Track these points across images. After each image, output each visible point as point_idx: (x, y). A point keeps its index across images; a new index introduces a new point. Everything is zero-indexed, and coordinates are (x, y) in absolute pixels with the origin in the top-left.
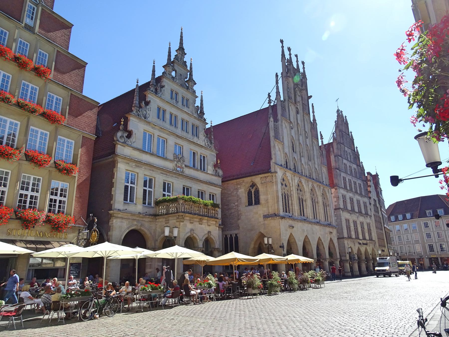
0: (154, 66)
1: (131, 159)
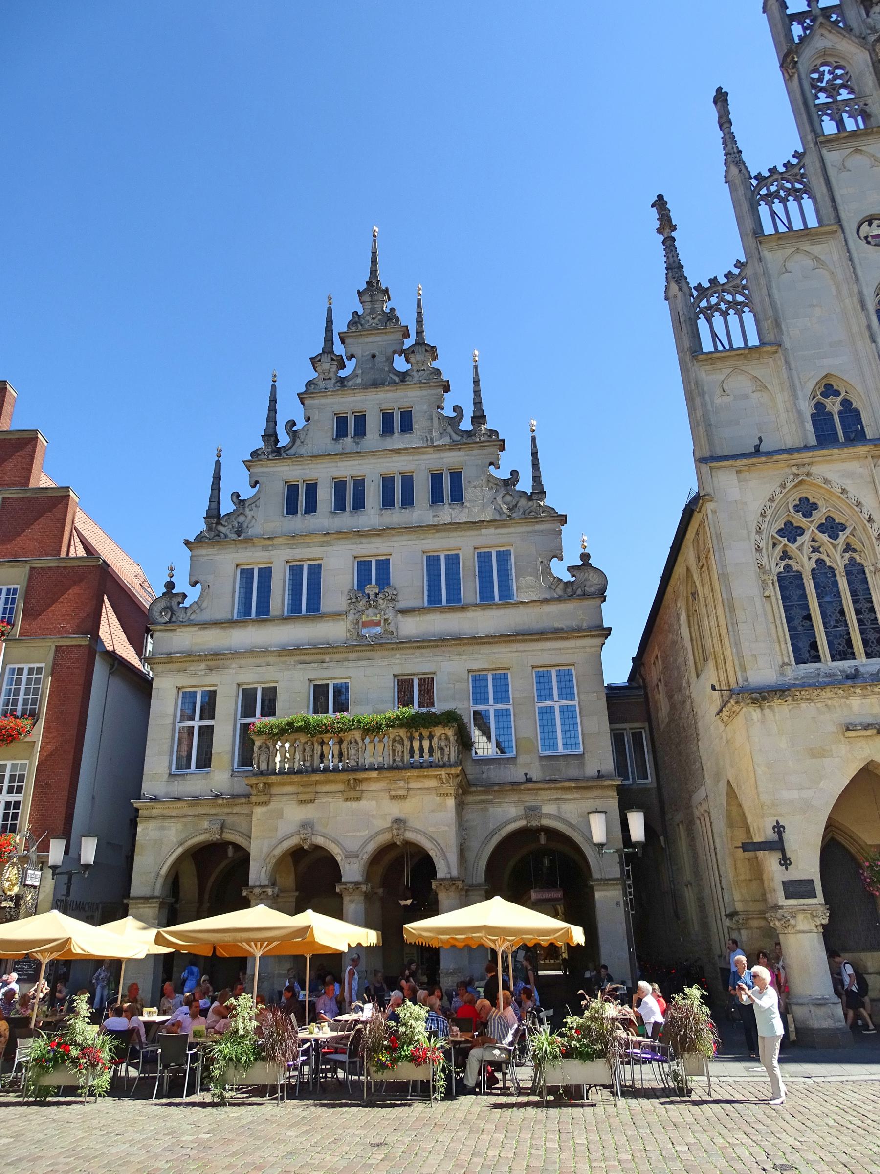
1: (189, 656)
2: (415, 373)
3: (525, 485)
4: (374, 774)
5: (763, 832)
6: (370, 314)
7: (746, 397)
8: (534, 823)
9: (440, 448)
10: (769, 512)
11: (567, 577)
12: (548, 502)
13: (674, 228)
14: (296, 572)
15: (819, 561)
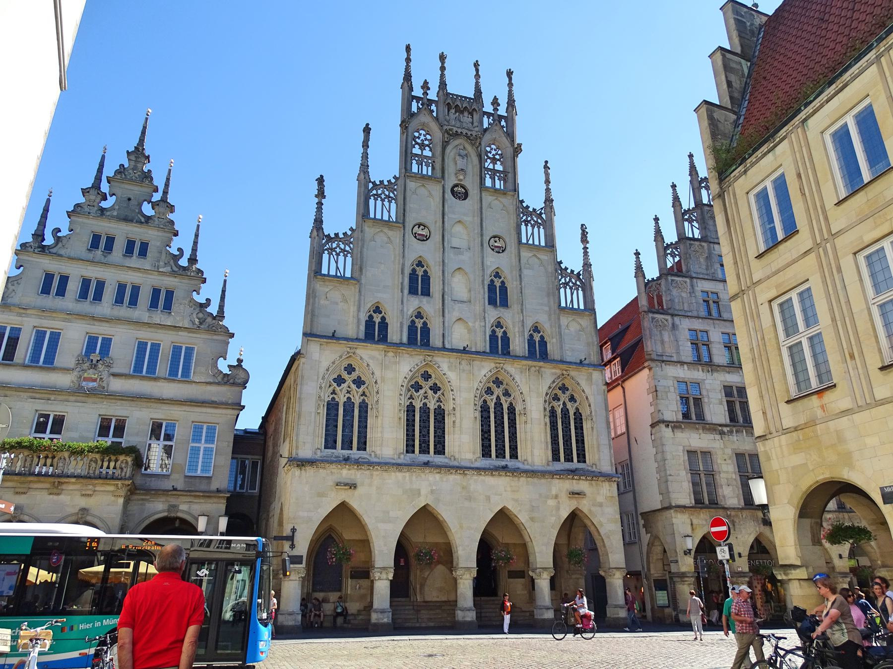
0: (48, 201)
2: (156, 219)
3: (213, 309)
4: (73, 480)
5: (287, 532)
6: (133, 169)
7: (337, 303)
8: (173, 515)
9: (163, 274)
10: (331, 369)
11: (226, 371)
12: (225, 323)
13: (324, 197)
14: (40, 335)
15: (349, 398)
